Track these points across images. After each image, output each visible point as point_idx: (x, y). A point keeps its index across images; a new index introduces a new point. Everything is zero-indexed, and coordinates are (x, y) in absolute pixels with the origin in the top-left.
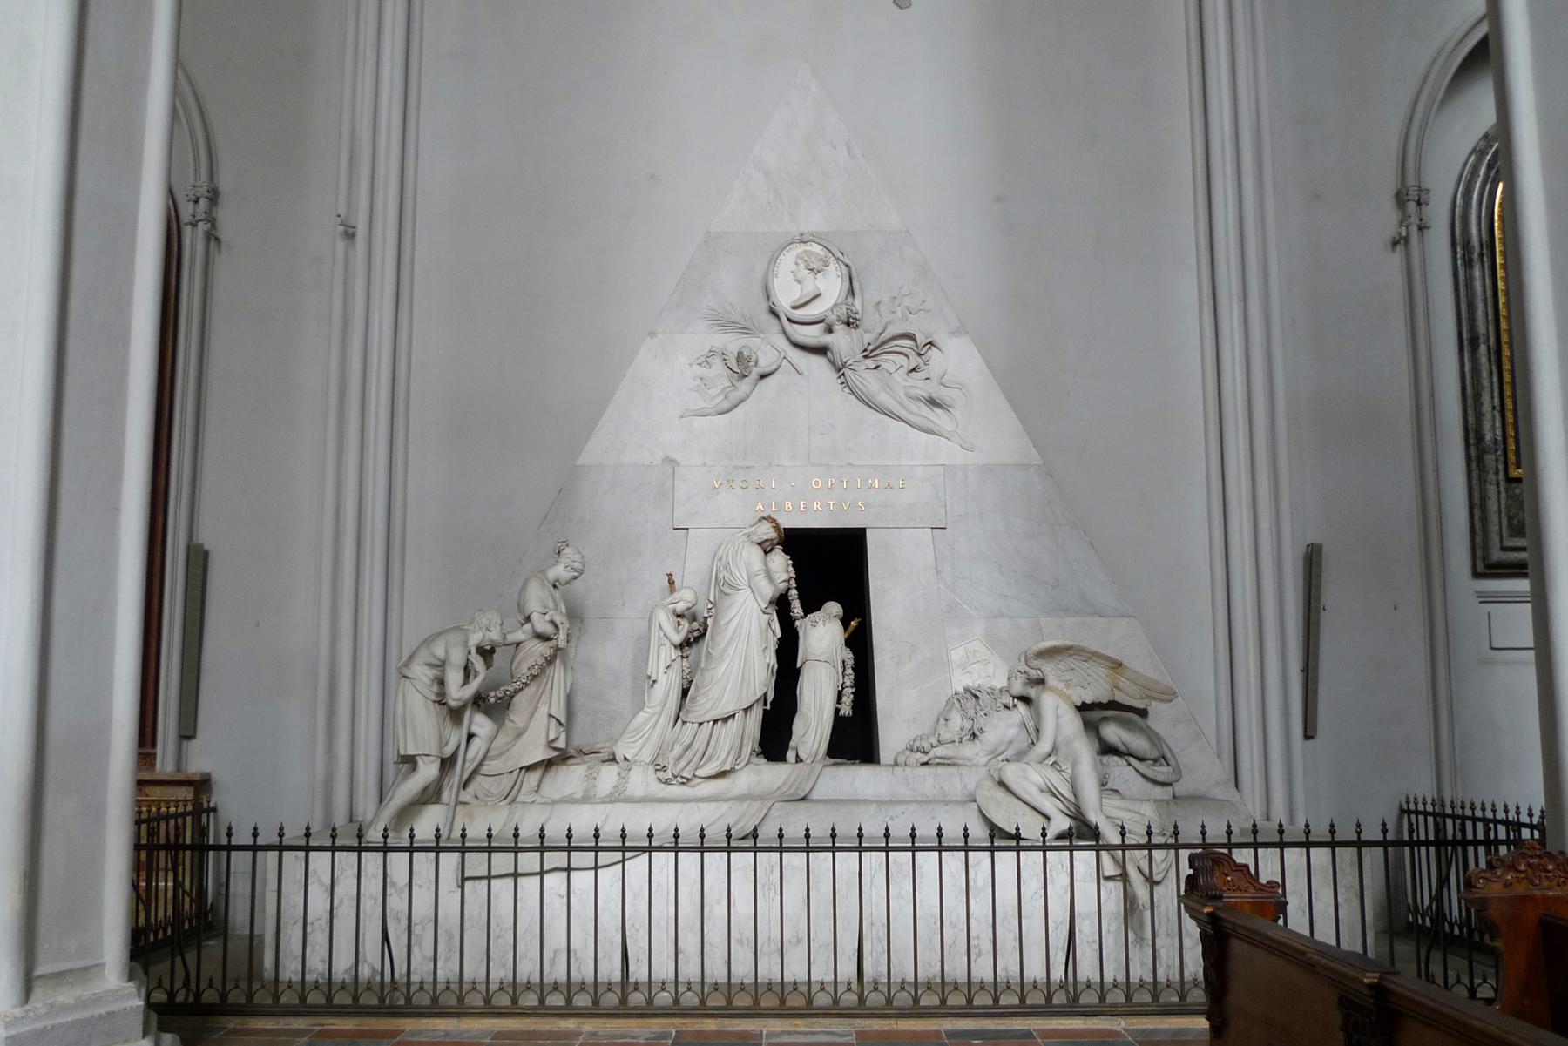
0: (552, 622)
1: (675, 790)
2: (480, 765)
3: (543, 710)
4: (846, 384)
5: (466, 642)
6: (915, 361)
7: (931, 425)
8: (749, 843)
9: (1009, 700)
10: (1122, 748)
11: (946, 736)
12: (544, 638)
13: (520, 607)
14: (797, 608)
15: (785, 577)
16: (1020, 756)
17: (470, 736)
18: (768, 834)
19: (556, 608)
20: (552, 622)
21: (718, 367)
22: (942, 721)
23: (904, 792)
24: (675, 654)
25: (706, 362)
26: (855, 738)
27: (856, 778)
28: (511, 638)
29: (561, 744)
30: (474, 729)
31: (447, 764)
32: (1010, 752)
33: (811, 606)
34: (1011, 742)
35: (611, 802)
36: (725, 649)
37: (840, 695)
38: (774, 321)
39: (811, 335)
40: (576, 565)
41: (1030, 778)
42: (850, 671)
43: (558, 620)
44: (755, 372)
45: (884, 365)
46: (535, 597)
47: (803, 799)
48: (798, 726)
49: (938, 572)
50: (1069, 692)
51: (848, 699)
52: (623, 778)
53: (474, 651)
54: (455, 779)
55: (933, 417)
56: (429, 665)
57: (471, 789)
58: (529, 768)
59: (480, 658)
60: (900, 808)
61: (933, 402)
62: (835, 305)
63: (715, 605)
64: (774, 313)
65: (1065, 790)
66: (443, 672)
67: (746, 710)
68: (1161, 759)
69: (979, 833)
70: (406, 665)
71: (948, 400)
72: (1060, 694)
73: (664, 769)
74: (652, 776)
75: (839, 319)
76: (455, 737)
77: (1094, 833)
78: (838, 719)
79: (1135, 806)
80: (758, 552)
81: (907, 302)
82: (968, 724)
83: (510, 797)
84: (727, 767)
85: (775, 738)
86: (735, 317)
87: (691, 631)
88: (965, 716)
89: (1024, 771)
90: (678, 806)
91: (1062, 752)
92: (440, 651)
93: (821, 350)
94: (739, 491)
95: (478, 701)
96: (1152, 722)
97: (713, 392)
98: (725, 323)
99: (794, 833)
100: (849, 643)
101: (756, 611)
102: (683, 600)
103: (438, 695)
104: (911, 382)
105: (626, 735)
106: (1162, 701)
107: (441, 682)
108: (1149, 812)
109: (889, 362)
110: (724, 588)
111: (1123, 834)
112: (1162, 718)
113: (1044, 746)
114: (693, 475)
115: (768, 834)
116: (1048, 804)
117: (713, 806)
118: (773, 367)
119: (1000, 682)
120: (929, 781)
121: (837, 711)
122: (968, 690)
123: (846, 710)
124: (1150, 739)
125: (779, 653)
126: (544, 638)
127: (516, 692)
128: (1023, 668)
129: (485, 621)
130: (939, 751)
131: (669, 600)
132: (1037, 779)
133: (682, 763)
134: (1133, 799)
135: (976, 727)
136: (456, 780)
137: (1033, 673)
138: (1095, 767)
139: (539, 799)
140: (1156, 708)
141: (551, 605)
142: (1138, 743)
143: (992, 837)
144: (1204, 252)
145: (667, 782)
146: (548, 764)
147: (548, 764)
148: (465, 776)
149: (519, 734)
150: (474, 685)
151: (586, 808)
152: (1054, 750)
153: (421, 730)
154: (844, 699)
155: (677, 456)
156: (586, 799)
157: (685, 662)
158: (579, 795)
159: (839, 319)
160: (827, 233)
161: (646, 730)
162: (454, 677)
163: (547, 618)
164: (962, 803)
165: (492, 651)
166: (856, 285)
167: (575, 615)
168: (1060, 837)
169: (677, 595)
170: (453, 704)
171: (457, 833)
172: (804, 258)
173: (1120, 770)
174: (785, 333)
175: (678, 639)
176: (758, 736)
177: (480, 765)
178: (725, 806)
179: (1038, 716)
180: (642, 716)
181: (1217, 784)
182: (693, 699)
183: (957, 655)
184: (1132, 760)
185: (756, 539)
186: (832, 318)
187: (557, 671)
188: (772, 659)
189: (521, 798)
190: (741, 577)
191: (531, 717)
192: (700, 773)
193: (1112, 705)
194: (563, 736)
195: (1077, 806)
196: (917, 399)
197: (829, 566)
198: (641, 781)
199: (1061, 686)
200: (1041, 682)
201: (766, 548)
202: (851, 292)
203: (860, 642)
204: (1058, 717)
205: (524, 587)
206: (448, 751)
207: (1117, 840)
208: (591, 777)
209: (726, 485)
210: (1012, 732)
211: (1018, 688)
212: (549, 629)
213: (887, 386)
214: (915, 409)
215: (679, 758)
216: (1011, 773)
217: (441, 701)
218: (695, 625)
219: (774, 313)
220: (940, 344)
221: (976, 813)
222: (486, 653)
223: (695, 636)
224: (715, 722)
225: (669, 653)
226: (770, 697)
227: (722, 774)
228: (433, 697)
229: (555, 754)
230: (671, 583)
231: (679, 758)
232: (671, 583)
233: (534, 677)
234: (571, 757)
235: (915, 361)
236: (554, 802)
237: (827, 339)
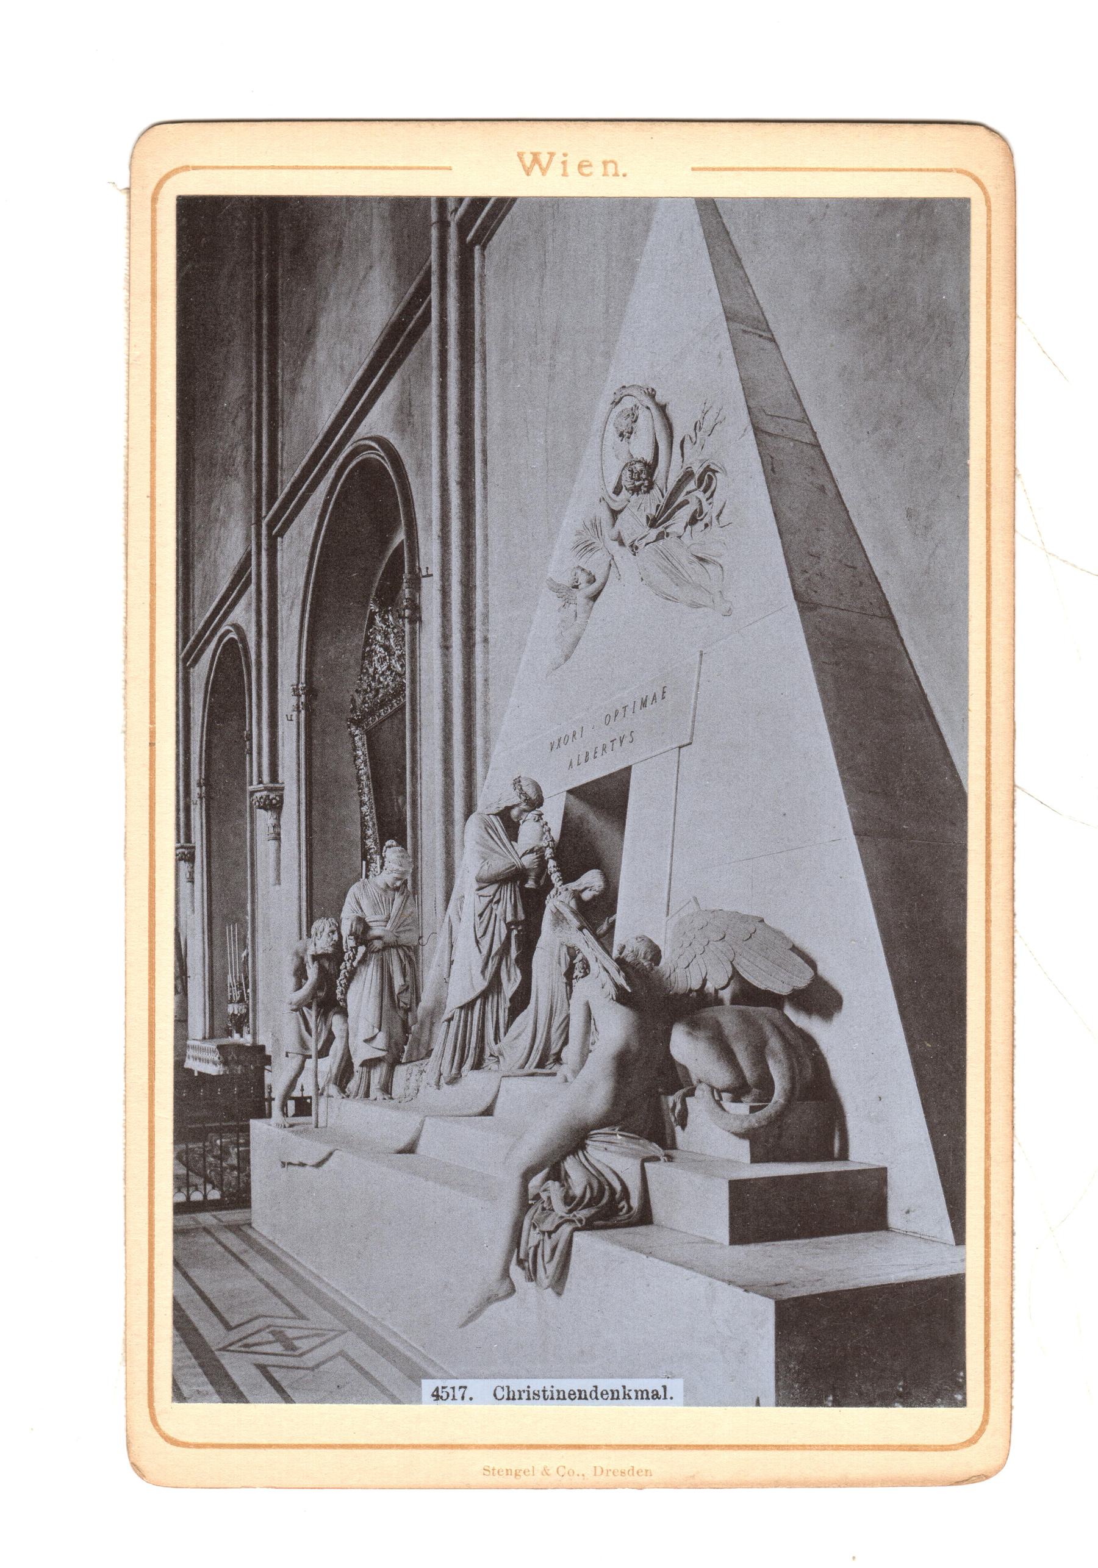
127: (345, 993)
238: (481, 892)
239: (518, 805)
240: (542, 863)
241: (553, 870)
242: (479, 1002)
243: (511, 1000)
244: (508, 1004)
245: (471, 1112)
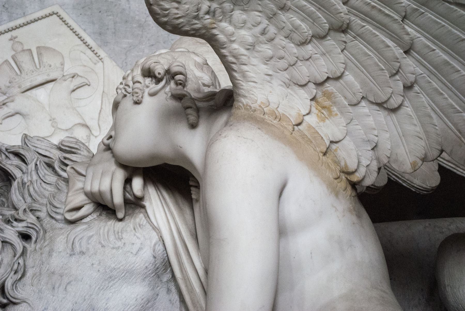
9: (110, 182)
50: (330, 129)
72: (290, 134)
137: (198, 64)
179: (204, 233)
199: (297, 104)
204: (282, 231)
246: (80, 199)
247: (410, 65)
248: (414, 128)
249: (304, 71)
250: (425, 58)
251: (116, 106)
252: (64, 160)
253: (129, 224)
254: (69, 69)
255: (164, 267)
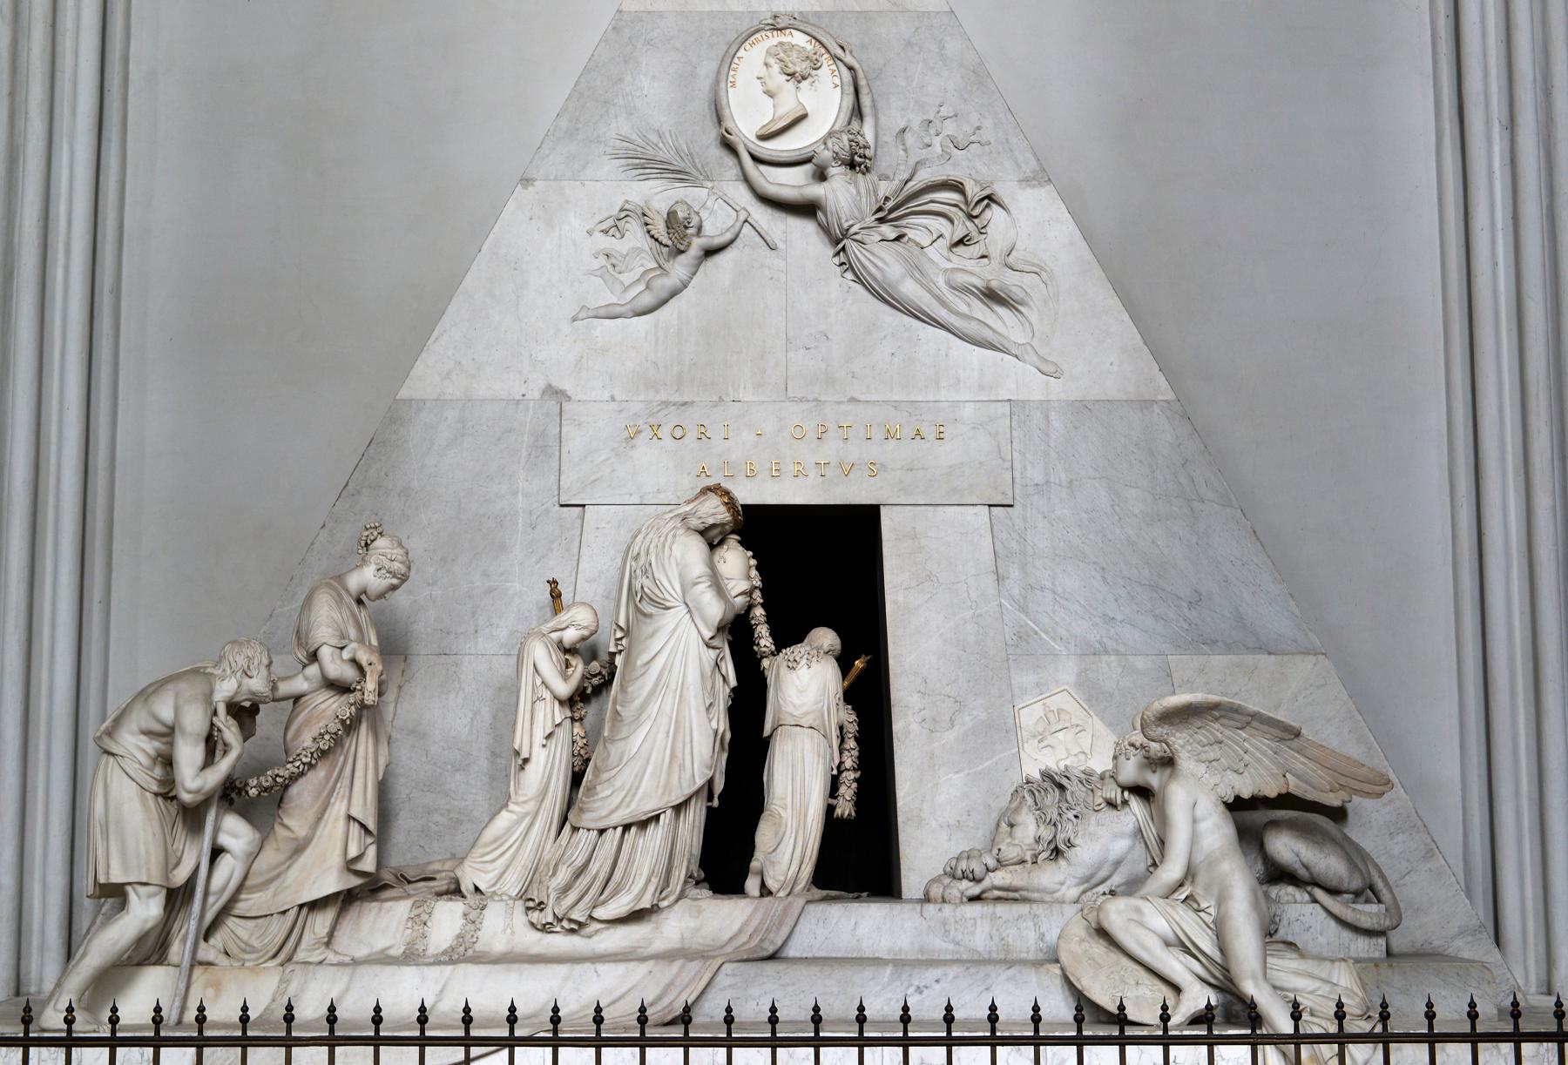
0: (354, 662)
1: (559, 942)
2: (234, 899)
3: (338, 809)
4: (847, 266)
5: (208, 697)
6: (962, 227)
7: (988, 335)
8: (677, 1032)
9: (1114, 793)
10: (1302, 872)
11: (1010, 853)
12: (339, 687)
13: (301, 636)
14: (765, 641)
15: (744, 586)
16: (1133, 886)
17: (217, 852)
18: (709, 1015)
19: (362, 639)
20: (354, 662)
21: (635, 236)
22: (1004, 826)
23: (939, 945)
24: (560, 714)
25: (615, 227)
26: (860, 856)
27: (861, 923)
28: (285, 688)
29: (368, 864)
30: (224, 840)
31: (177, 898)
32: (1117, 880)
33: (788, 634)
34: (1118, 863)
35: (452, 962)
36: (643, 707)
37: (835, 784)
38: (729, 160)
39: (789, 183)
40: (396, 566)
41: (1147, 923)
42: (851, 744)
43: (364, 658)
44: (695, 250)
45: (911, 234)
46: (327, 621)
47: (773, 957)
48: (764, 835)
49: (999, 579)
51: (847, 791)
52: (472, 921)
53: (222, 710)
54: (188, 926)
55: (991, 320)
56: (148, 733)
57: (217, 940)
58: (315, 906)
59: (232, 722)
60: (932, 974)
61: (992, 296)
62: (830, 134)
63: (627, 632)
64: (729, 147)
65: (1206, 944)
66: (171, 744)
67: (679, 809)
68: (1368, 892)
69: (1058, 1010)
70: (110, 733)
71: (1017, 293)
73: (541, 906)
74: (520, 918)
75: (836, 157)
76: (191, 856)
77: (1251, 1015)
78: (832, 825)
79: (1323, 970)
80: (694, 549)
81: (950, 128)
82: (1047, 833)
83: (284, 954)
84: (646, 903)
85: (725, 860)
86: (664, 154)
87: (584, 678)
88: (1041, 820)
89: (1138, 910)
90: (562, 969)
91: (1202, 878)
92: (166, 711)
93: (807, 209)
94: (668, 442)
95: (230, 794)
96: (1353, 831)
97: (626, 278)
98: (645, 164)
99: (751, 1012)
100: (850, 696)
101: (695, 644)
102: (575, 624)
103: (161, 782)
104: (956, 262)
105: (478, 851)
106: (1367, 794)
107: (167, 761)
108: (1344, 979)
109: (921, 229)
110: (641, 603)
111: (1296, 1016)
112: (1371, 825)
113: (1172, 870)
114: (592, 415)
115: (709, 1015)
116: (1177, 966)
117: (621, 968)
118: (728, 236)
119: (1101, 763)
120: (979, 928)
121: (830, 809)
122: (1047, 776)
123: (845, 808)
124: (1350, 861)
125: (734, 713)
126: (339, 687)
127: (294, 778)
128: (1139, 738)
129: (241, 661)
130: (1000, 878)
131: (551, 625)
132: (1160, 924)
133: (572, 897)
134: (1320, 958)
135: (1061, 837)
136: (193, 924)
138: (1256, 906)
139: (332, 958)
140: (1360, 806)
141: (353, 633)
142: (1329, 864)
143: (1079, 1020)
144: (1445, 48)
145: (545, 928)
146: (345, 900)
147: (345, 900)
148: (209, 917)
149: (299, 848)
150: (223, 766)
151: (409, 974)
152: (1190, 874)
153: (132, 839)
154: (842, 789)
155: (566, 385)
156: (411, 957)
157: (577, 729)
158: (397, 951)
159: (836, 157)
160: (817, 14)
161: (512, 840)
162: (189, 754)
163: (346, 655)
164: (1037, 964)
165: (254, 709)
166: (866, 101)
167: (394, 648)
168: (1195, 1021)
169: (564, 618)
170: (186, 797)
171: (191, 1015)
172: (780, 54)
173: (1303, 914)
174: (746, 180)
175: (564, 689)
176: (697, 851)
177: (234, 899)
178: (641, 970)
179: (1161, 819)
180: (504, 819)
181: (1462, 933)
182: (591, 789)
183: (1030, 717)
184: (1319, 894)
185: (695, 523)
186: (826, 155)
187: (363, 742)
188: (721, 723)
189: (301, 955)
190: (671, 587)
191: (319, 819)
192: (600, 913)
193: (1287, 801)
194: (372, 852)
195: (1226, 969)
196: (964, 290)
197: (816, 568)
198: (503, 927)
200: (1168, 762)
201: (713, 539)
202: (857, 112)
203: (869, 696)
204: (1195, 821)
205: (308, 603)
206: (180, 876)
207: (1287, 1027)
208: (419, 921)
209: (648, 433)
210: (1120, 846)
211: (1130, 771)
212: (349, 673)
213: (916, 270)
214: (963, 308)
215: (566, 889)
216: (1117, 915)
217: (167, 792)
218: (595, 666)
219: (729, 147)
220: (1006, 200)
221: (1058, 981)
222: (244, 713)
223: (595, 683)
224: (627, 827)
225: (549, 714)
226: (719, 786)
227: (636, 916)
228: (155, 788)
229: (356, 882)
230: (556, 596)
231: (566, 889)
232: (556, 596)
233: (324, 754)
234: (386, 887)
235: (962, 227)
236: (355, 963)
237: (817, 191)
238: (715, 643)
239: (722, 525)
240: (750, 607)
241: (763, 619)
242: (693, 802)
243: (720, 797)
244: (716, 803)
245: (765, 954)
246: (1100, 800)
247: (1246, 757)
248: (1248, 781)
249: (1204, 757)
250: (1253, 755)
251: (1115, 757)
252: (1087, 778)
253: (1122, 813)
254: (1075, 721)
255: (1139, 832)
